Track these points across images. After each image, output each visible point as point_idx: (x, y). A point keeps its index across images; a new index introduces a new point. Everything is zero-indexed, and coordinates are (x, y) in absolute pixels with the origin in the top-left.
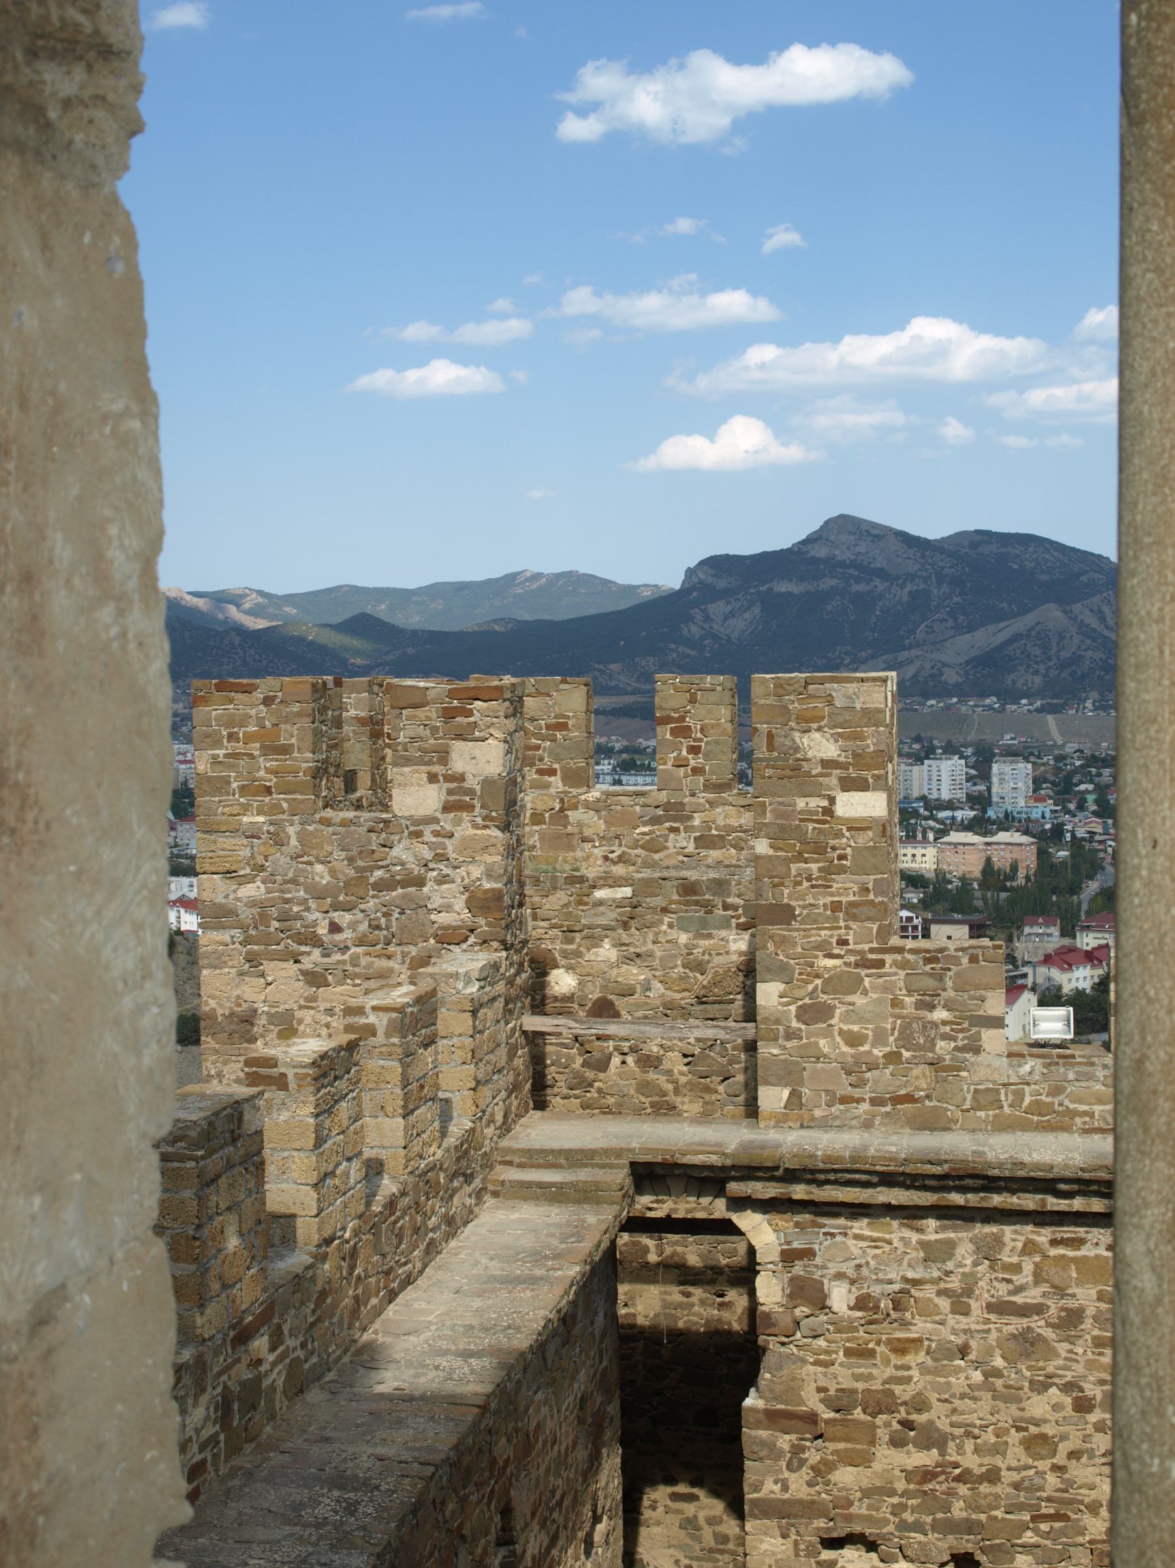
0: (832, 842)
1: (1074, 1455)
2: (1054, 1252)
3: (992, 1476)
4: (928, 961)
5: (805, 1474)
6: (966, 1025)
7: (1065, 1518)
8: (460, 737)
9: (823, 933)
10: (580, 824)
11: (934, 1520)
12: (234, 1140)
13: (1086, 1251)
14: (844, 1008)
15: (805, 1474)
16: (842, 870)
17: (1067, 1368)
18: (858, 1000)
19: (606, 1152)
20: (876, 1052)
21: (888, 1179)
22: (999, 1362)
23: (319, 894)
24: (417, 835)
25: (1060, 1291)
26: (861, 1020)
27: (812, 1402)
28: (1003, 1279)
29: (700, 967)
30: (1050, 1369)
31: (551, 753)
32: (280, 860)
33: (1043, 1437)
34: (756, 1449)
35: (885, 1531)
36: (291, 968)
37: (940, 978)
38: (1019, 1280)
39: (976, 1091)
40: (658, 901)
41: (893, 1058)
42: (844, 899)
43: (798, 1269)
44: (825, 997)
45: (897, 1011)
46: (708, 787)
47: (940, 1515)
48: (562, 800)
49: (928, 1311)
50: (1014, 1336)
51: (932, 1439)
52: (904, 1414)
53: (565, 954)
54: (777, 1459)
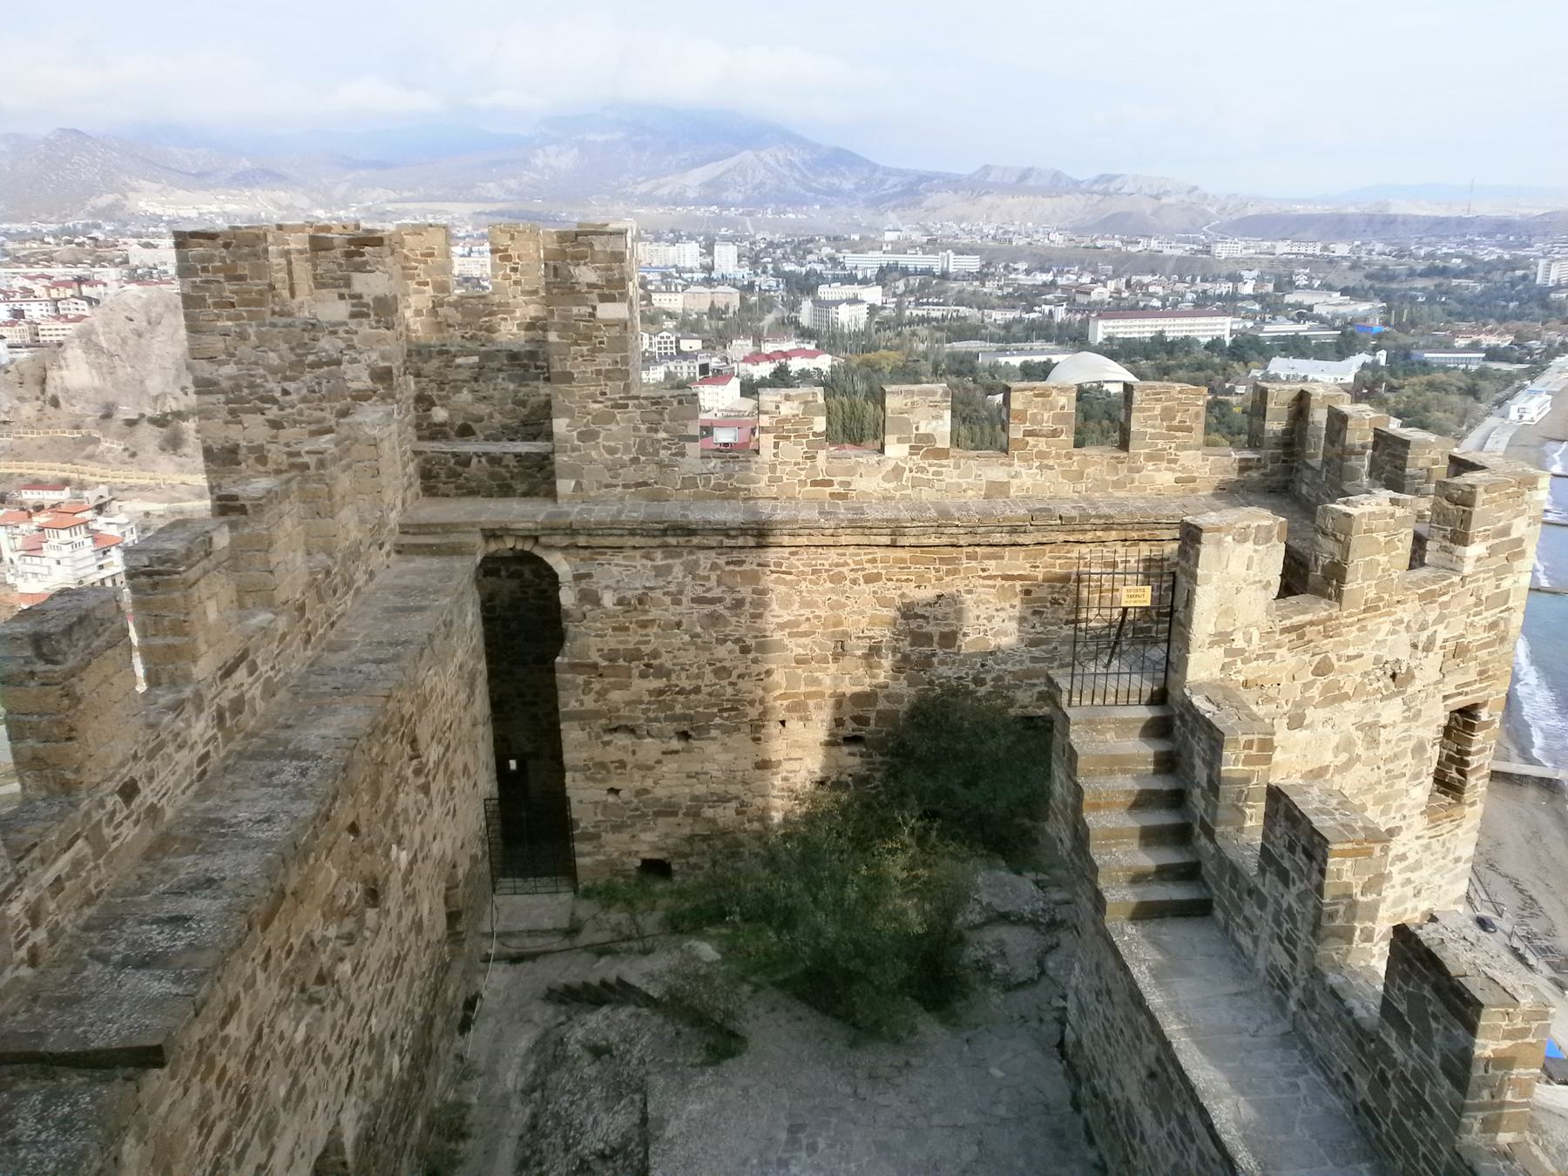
1: (739, 676)
2: (728, 568)
3: (697, 690)
4: (653, 404)
5: (593, 696)
10: (446, 317)
12: (208, 554)
13: (746, 567)
15: (593, 696)
16: (602, 350)
18: (614, 427)
19: (466, 524)
21: (632, 533)
22: (699, 630)
23: (273, 371)
25: (732, 590)
26: (616, 439)
27: (595, 657)
29: (523, 404)
31: (425, 272)
32: (244, 350)
33: (724, 668)
36: (259, 418)
37: (661, 414)
40: (495, 365)
41: (635, 460)
43: (583, 584)
46: (524, 293)
49: (658, 604)
51: (662, 672)
53: (440, 398)
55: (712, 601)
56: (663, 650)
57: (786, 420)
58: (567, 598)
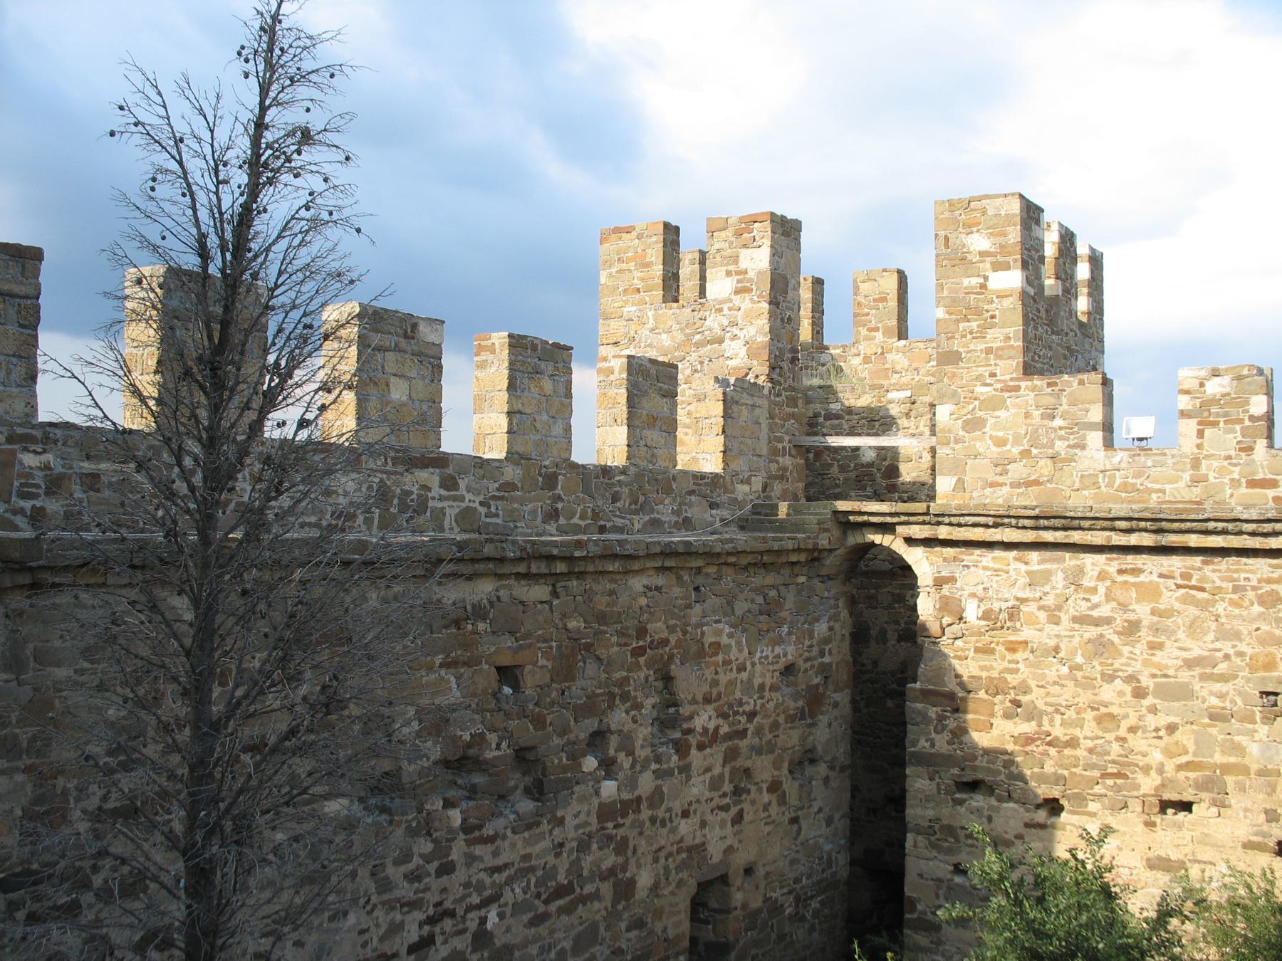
0: (986, 307)
1: (1132, 730)
2: (1120, 578)
3: (1073, 743)
5: (946, 736)
6: (1076, 429)
7: (1125, 777)
8: (745, 246)
9: (980, 369)
11: (1033, 772)
14: (993, 420)
16: (993, 326)
17: (1128, 665)
18: (1002, 414)
20: (1014, 450)
24: (720, 310)
25: (1124, 607)
28: (1084, 599)
30: (1116, 666)
33: (1111, 716)
34: (914, 716)
35: (998, 779)
38: (1095, 599)
39: (1082, 476)
41: (1026, 454)
42: (994, 345)
43: (946, 590)
44: (981, 413)
45: (1028, 421)
47: (1036, 770)
48: (882, 347)
49: (1032, 621)
50: (1090, 641)
51: (1033, 714)
52: (1013, 695)
54: (928, 724)
55: (1097, 622)
56: (1033, 683)
57: (1213, 401)
58: (926, 607)
